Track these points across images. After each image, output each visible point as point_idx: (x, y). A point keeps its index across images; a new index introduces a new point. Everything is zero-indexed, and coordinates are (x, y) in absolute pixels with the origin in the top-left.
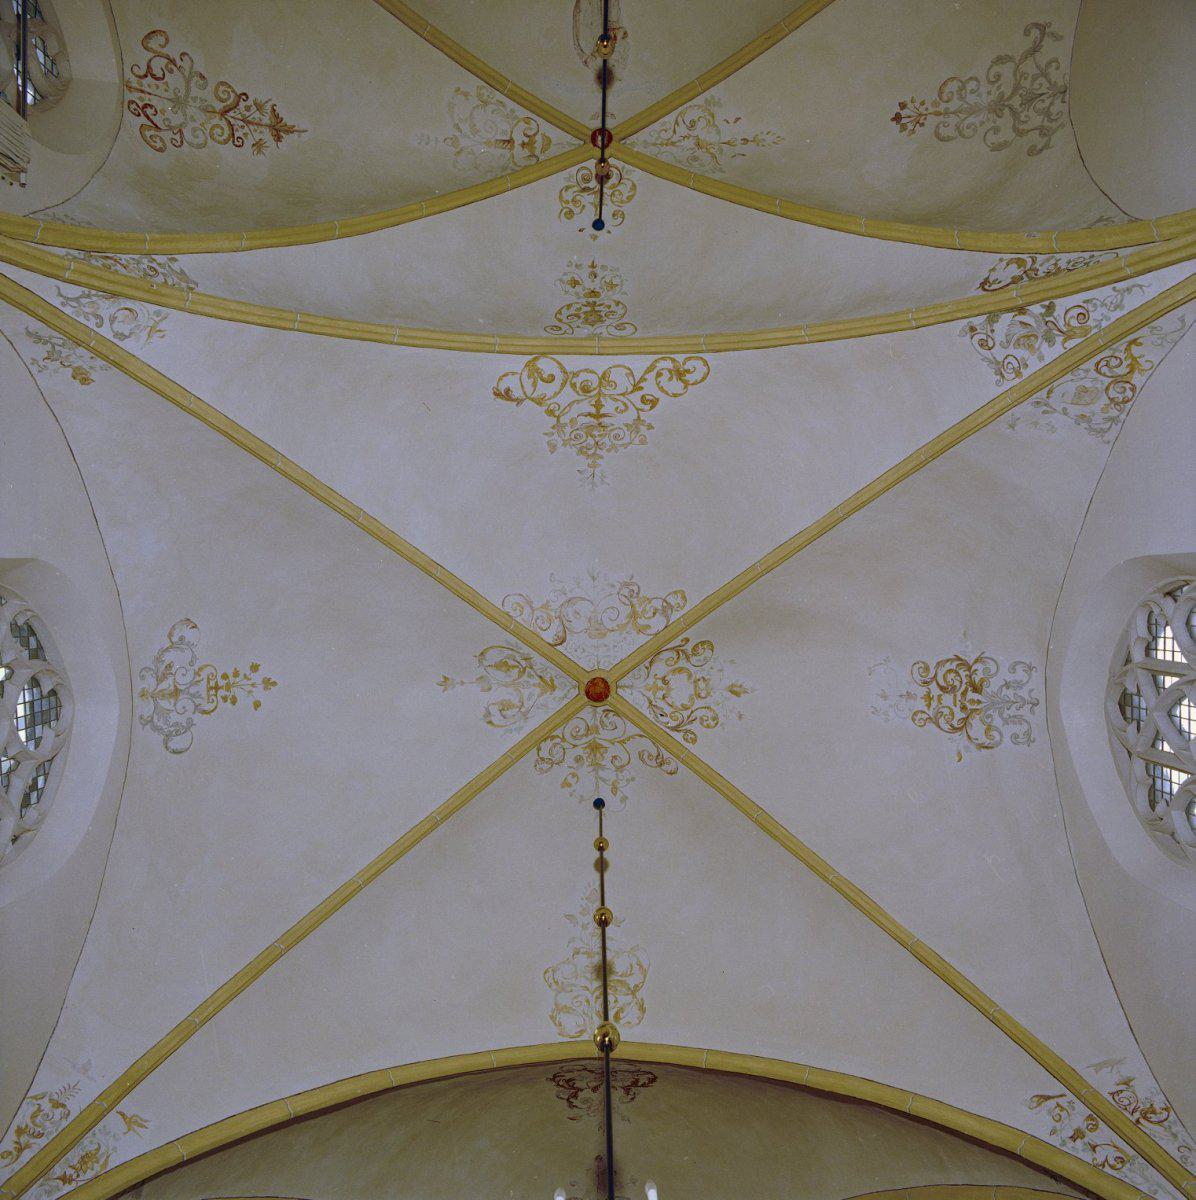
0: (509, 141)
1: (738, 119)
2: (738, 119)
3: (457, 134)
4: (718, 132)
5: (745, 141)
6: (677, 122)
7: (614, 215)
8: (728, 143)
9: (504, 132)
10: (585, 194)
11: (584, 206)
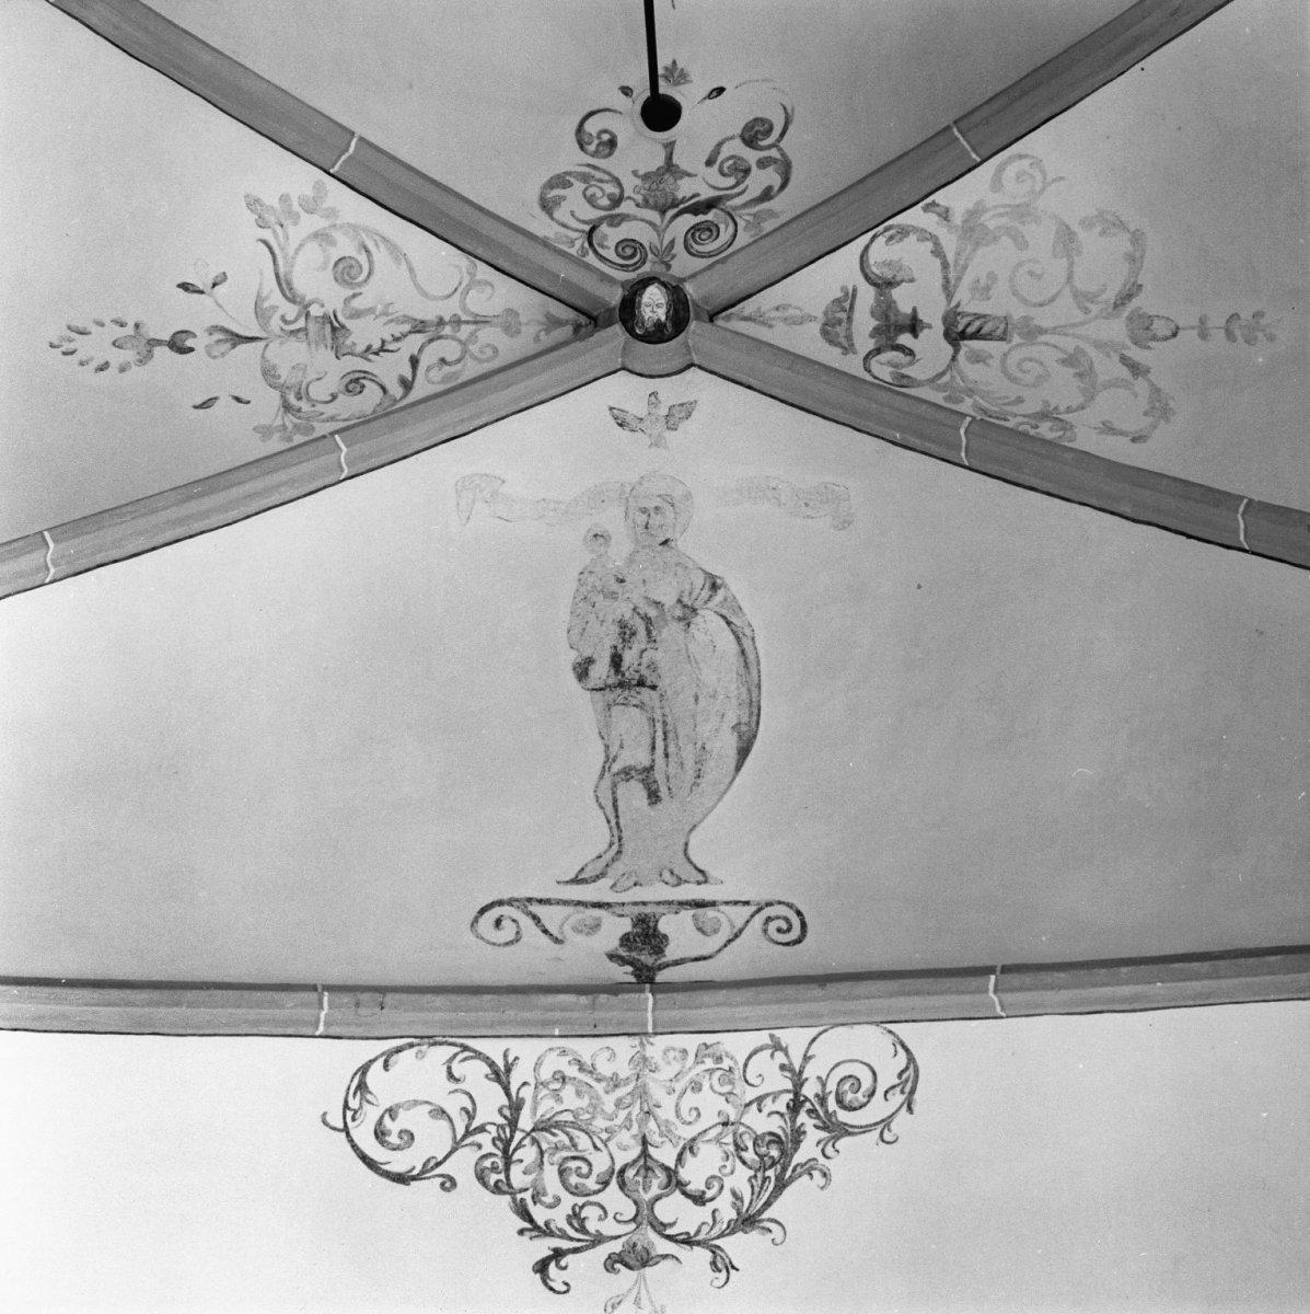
0: (963, 335)
1: (205, 405)
2: (205, 405)
3: (1135, 353)
4: (269, 373)
5: (179, 345)
6: (407, 385)
7: (612, 143)
8: (238, 339)
9: (977, 358)
10: (706, 194)
11: (709, 163)
